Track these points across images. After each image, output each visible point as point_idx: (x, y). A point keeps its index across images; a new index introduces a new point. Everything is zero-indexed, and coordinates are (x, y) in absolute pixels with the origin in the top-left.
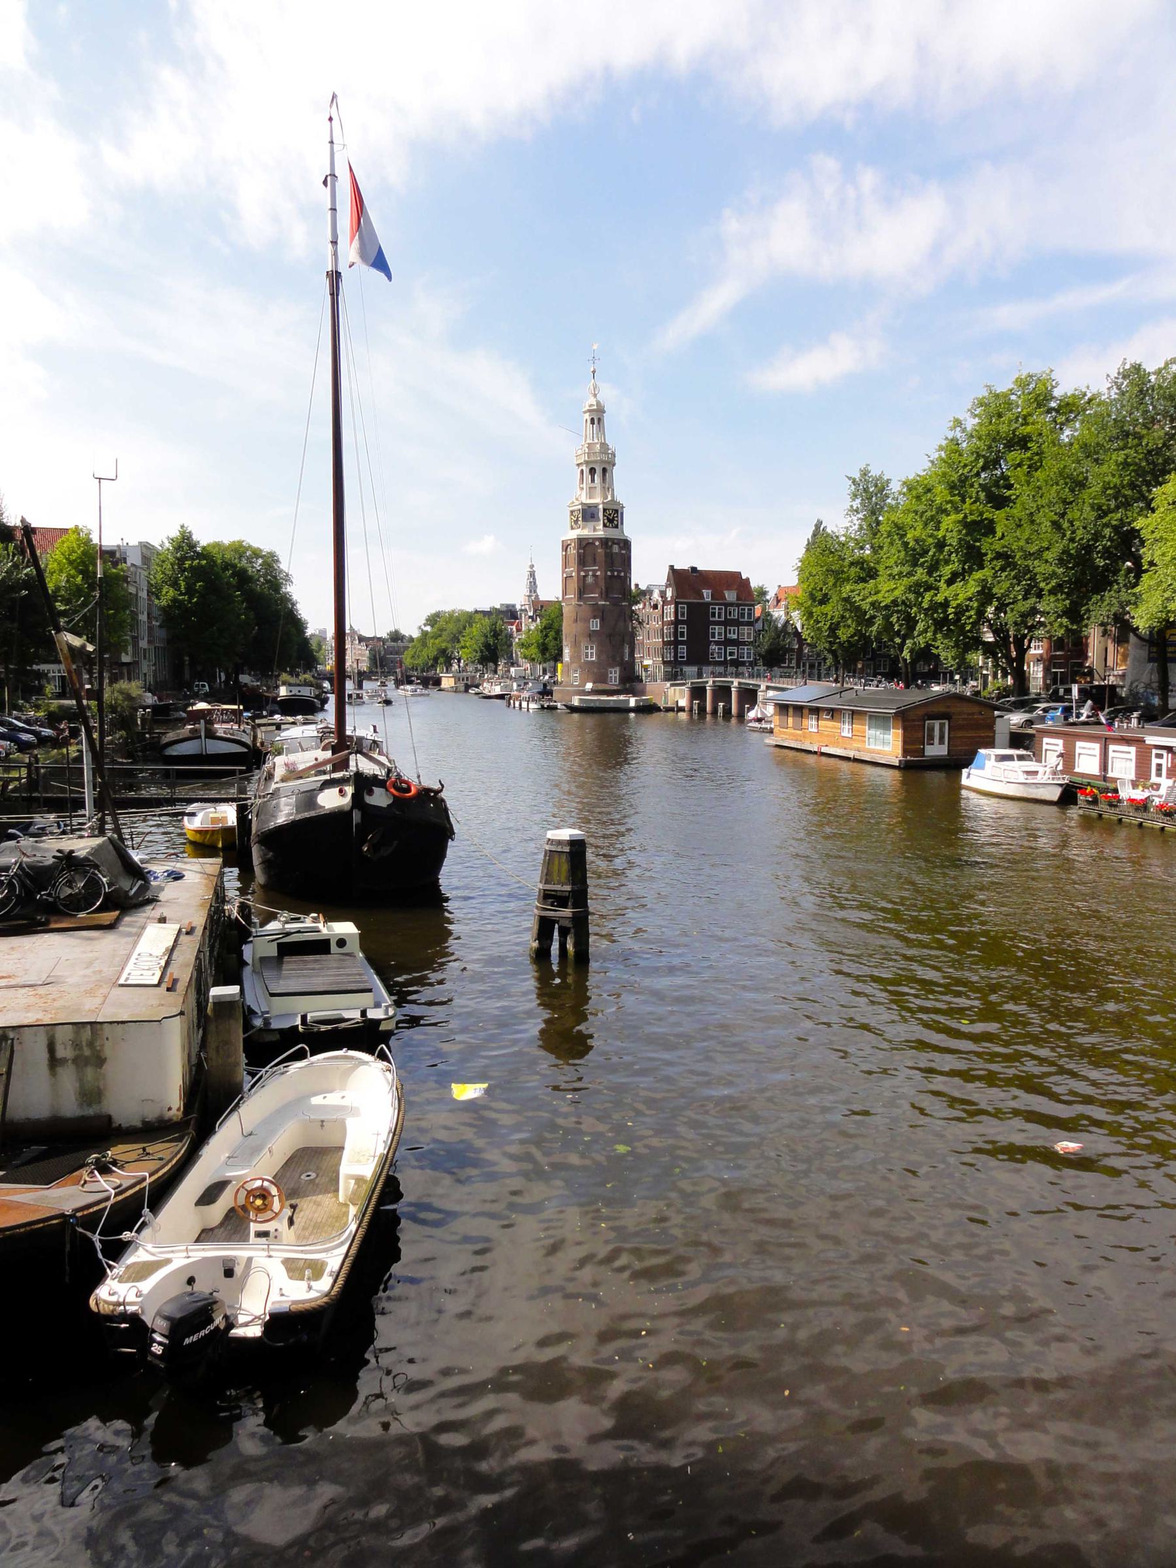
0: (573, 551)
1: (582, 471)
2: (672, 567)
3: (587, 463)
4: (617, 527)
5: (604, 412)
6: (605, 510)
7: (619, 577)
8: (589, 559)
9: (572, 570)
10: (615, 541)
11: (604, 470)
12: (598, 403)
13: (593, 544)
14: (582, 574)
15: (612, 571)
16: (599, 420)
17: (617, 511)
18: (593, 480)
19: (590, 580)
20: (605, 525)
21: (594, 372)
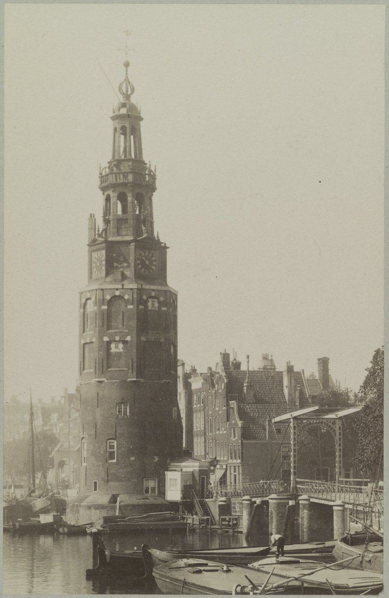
0: (91, 308)
1: (108, 199)
3: (114, 186)
9: (91, 334)
12: (133, 108)
14: (106, 339)
18: (124, 210)
21: (127, 65)
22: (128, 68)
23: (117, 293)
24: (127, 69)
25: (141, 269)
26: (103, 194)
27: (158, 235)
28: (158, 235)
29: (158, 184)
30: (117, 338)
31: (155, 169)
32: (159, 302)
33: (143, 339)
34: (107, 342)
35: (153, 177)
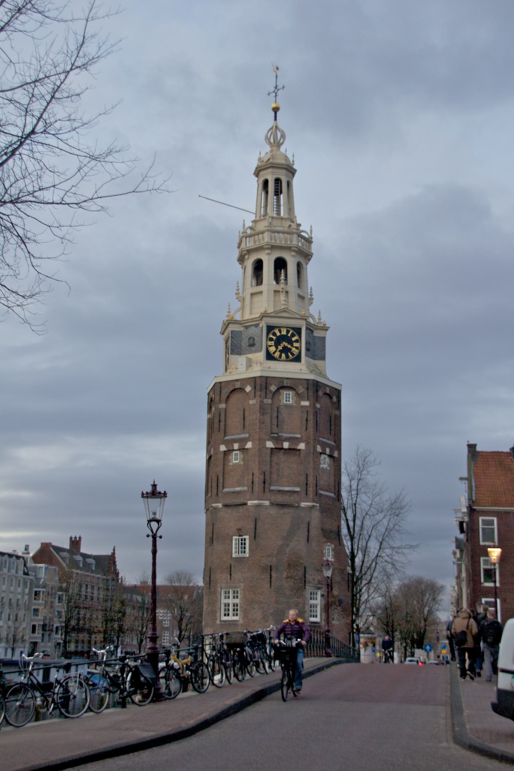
2: (472, 447)
4: (298, 359)
5: (291, 171)
6: (270, 328)
7: (292, 450)
8: (234, 420)
10: (285, 385)
11: (280, 265)
13: (242, 389)
14: (223, 448)
15: (278, 440)
16: (278, 181)
17: (298, 331)
19: (236, 459)
20: (270, 357)
21: (276, 110)
22: (278, 113)
23: (238, 385)
24: (276, 113)
25: (274, 353)
26: (242, 268)
27: (320, 316)
28: (320, 316)
29: (314, 248)
30: (236, 446)
31: (311, 231)
32: (298, 394)
33: (270, 444)
34: (225, 451)
35: (309, 241)
